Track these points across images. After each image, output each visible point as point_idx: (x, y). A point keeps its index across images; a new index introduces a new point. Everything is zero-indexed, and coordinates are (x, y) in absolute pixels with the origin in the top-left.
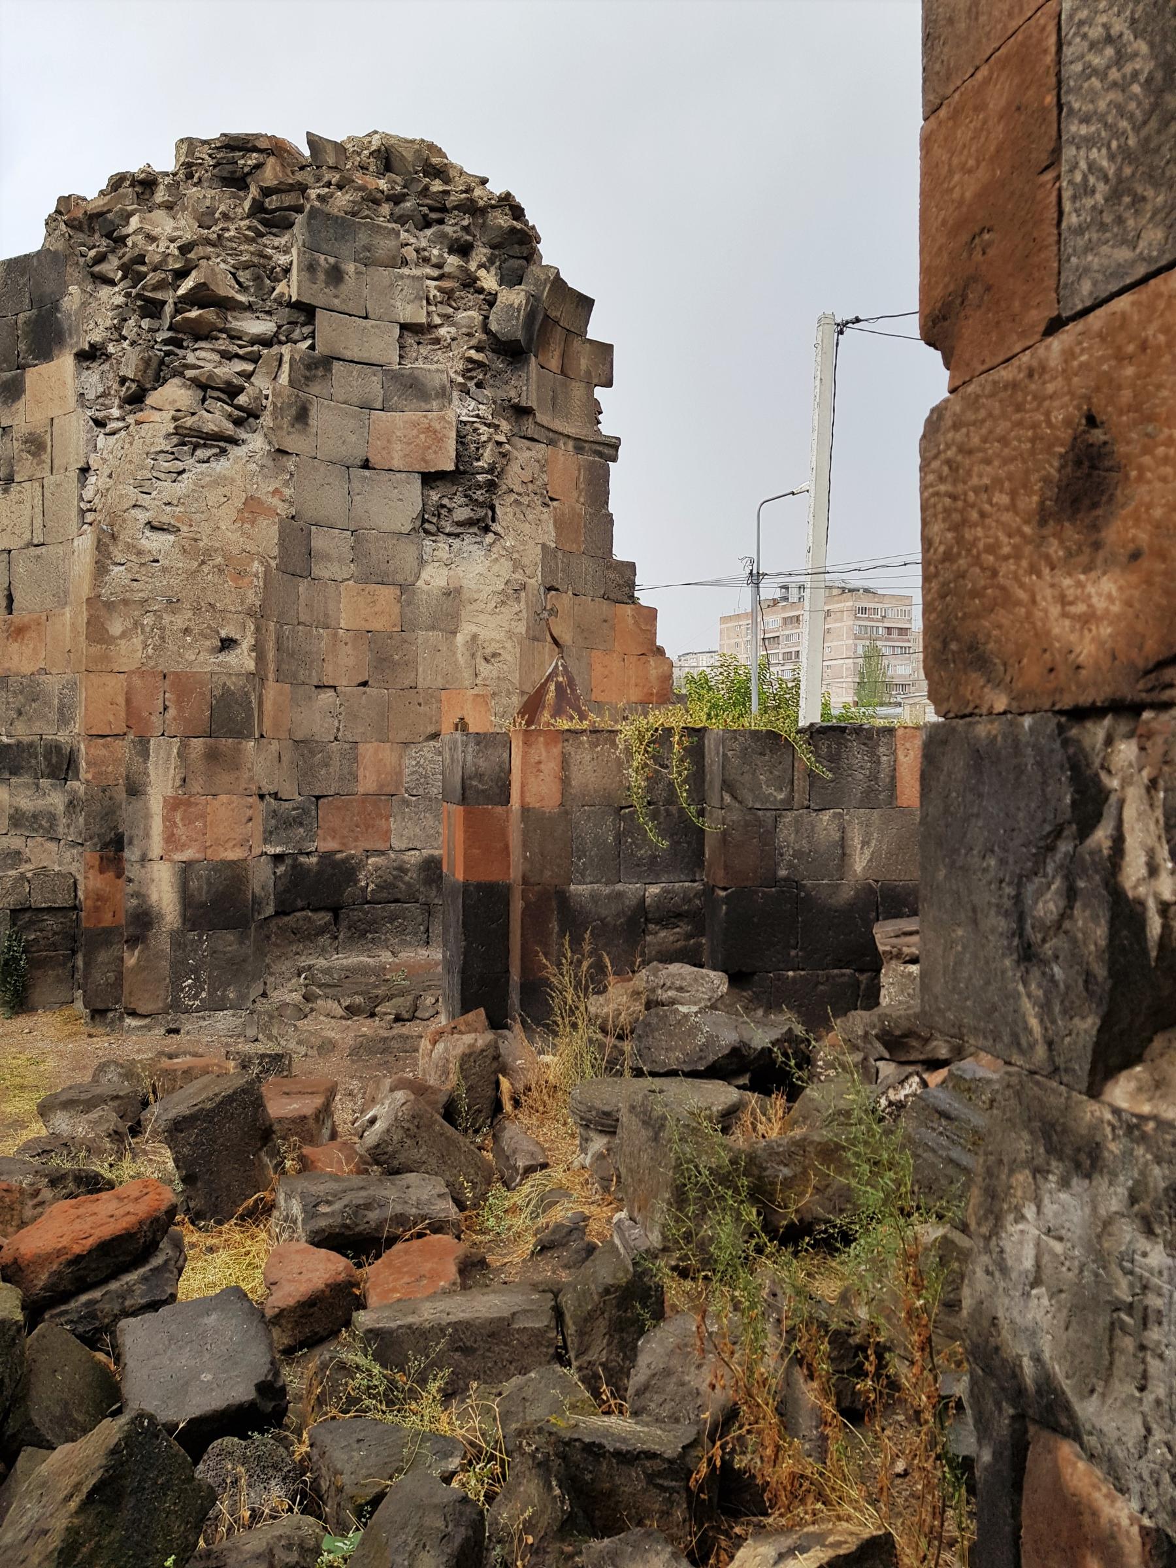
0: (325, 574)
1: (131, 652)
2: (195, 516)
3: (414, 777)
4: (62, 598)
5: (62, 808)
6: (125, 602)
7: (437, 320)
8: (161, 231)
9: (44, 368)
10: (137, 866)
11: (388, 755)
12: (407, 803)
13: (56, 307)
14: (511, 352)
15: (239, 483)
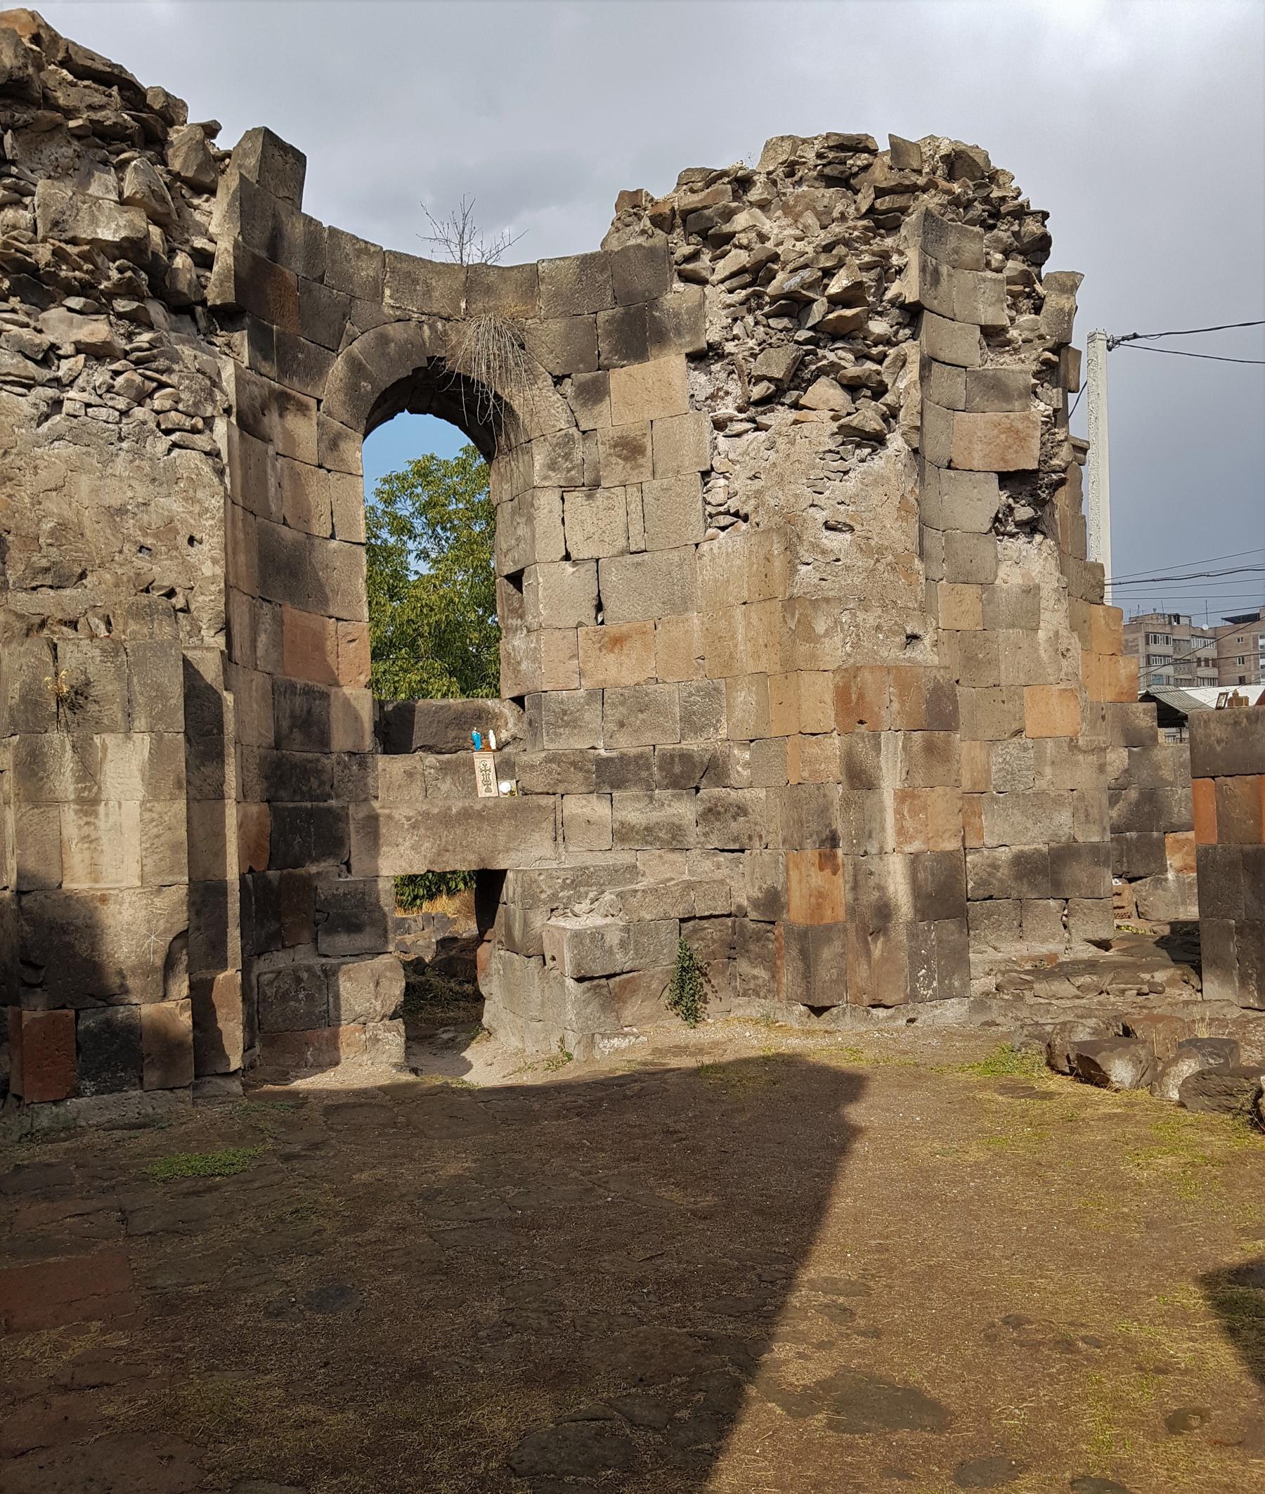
1: (835, 650)
2: (864, 515)
3: (1001, 774)
4: (681, 604)
5: (691, 817)
9: (635, 369)
10: (876, 859)
12: (994, 799)
15: (893, 481)
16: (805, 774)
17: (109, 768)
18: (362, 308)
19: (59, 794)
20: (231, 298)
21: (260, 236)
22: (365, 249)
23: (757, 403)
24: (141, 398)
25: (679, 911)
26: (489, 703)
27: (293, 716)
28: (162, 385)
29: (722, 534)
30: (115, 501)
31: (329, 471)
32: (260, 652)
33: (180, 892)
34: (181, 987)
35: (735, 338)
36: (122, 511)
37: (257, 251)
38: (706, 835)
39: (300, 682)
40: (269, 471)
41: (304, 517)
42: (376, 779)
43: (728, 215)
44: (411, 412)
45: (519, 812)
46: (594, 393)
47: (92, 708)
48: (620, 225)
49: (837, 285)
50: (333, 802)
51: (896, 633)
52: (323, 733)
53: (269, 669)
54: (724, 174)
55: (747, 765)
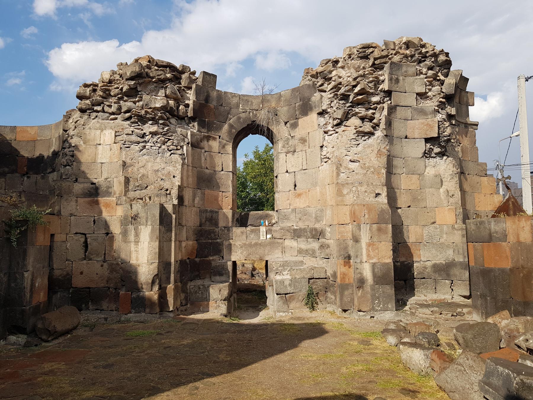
0: (397, 172)
1: (350, 199)
4: (315, 184)
5: (317, 247)
6: (347, 184)
7: (427, 91)
8: (345, 75)
9: (305, 118)
11: (418, 229)
13: (309, 100)
14: (449, 99)
16: (340, 237)
17: (142, 234)
18: (234, 111)
19: (130, 240)
20: (192, 115)
21: (202, 98)
22: (234, 95)
23: (337, 125)
24: (164, 143)
25: (309, 276)
26: (270, 212)
27: (206, 218)
28: (169, 139)
29: (325, 164)
30: (156, 169)
32: (196, 201)
33: (156, 265)
34: (156, 288)
35: (332, 107)
36: (158, 171)
38: (321, 253)
39: (209, 209)
40: (202, 156)
41: (213, 166)
42: (232, 234)
43: (330, 72)
44: (252, 134)
45: (273, 243)
46: (295, 126)
47: (139, 219)
48: (304, 78)
49: (357, 90)
50: (218, 240)
51: (371, 193)
52: (216, 222)
54: (329, 61)
55: (329, 232)
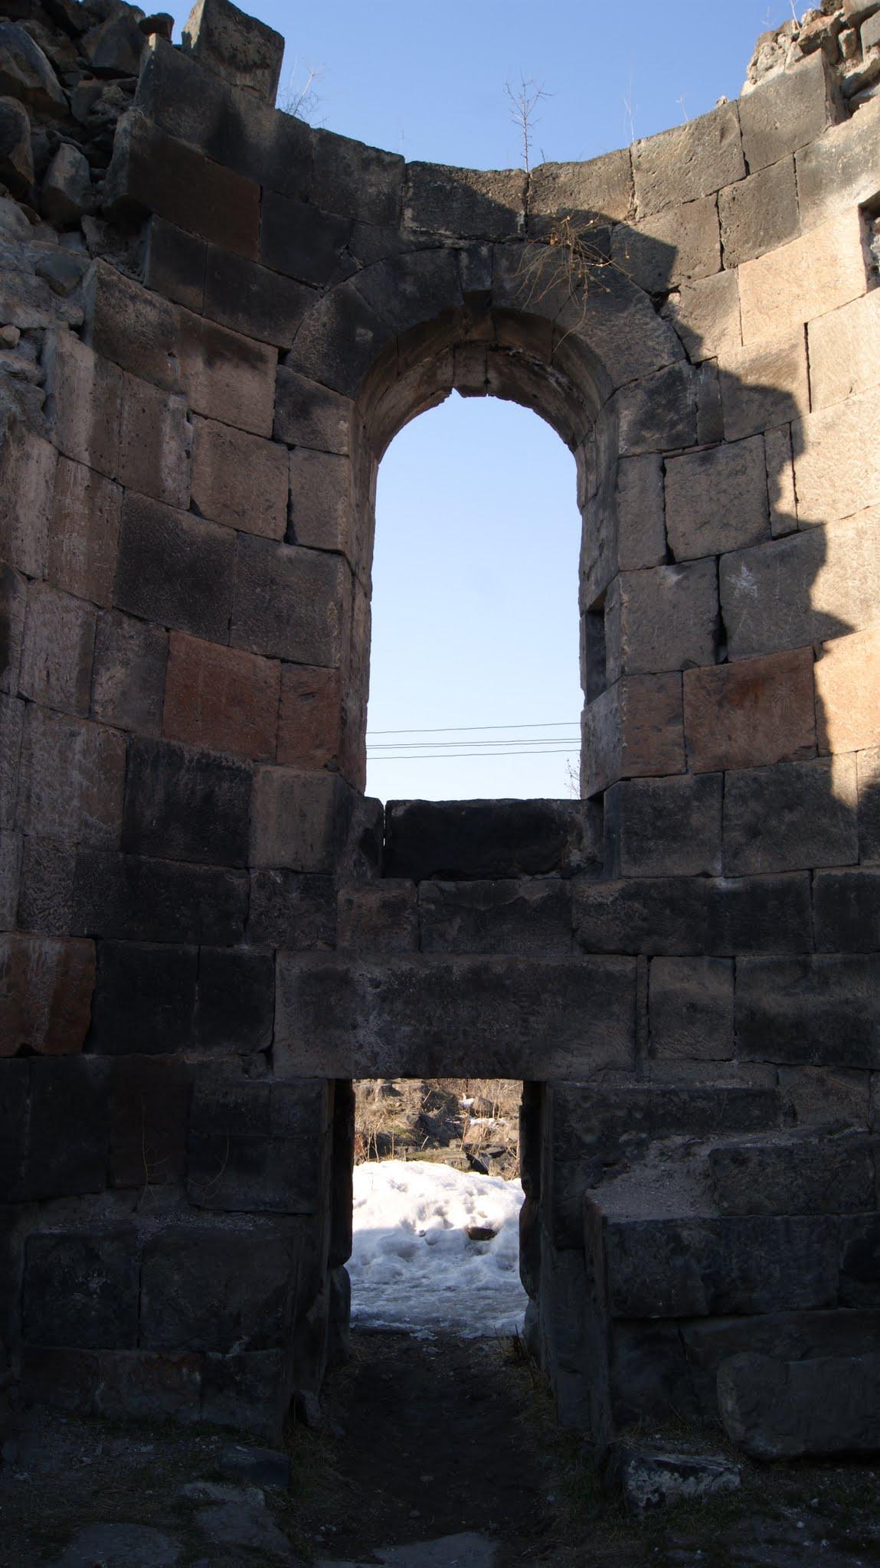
9: (779, 254)
31: (291, 447)
37: (185, 142)
39: (193, 750)
40: (167, 428)
44: (467, 391)
53: (127, 722)
